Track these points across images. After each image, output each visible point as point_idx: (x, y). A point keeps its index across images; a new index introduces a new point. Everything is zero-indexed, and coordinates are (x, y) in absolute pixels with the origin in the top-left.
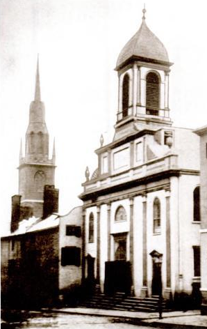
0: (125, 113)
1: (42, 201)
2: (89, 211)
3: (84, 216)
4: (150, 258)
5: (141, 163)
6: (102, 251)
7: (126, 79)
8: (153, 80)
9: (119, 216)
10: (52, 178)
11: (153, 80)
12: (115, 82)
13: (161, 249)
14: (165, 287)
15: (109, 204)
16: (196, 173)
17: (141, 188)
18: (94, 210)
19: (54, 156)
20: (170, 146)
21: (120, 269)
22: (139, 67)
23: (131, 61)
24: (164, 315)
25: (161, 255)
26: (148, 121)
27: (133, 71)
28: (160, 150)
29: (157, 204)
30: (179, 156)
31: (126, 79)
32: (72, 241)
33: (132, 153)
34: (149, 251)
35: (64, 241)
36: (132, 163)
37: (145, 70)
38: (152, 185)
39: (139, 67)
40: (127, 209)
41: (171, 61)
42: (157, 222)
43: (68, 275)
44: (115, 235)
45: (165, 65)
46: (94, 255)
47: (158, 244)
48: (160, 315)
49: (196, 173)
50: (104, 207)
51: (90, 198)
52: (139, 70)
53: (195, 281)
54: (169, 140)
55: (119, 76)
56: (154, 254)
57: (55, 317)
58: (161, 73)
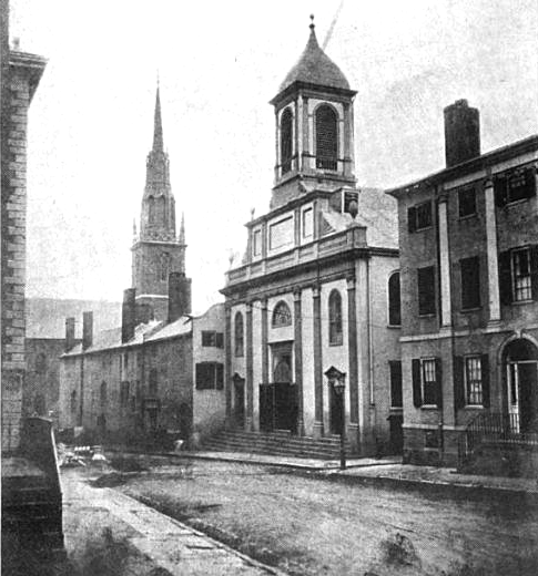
0: (286, 168)
1: (167, 297)
2: (235, 310)
3: (229, 318)
4: (325, 379)
5: (311, 240)
6: (259, 369)
7: (288, 114)
8: (327, 120)
9: (279, 317)
10: (180, 263)
11: (327, 120)
12: (269, 121)
13: (344, 367)
14: (348, 424)
15: (265, 300)
16: (393, 254)
17: (312, 276)
18: (243, 309)
19: (183, 231)
20: (354, 213)
21: (282, 401)
22: (306, 99)
23: (294, 90)
24: (348, 463)
25: (344, 375)
26: (319, 179)
27: (296, 104)
28: (339, 222)
29: (335, 298)
30: (369, 230)
31: (288, 114)
32: (210, 355)
33: (297, 226)
34: (325, 370)
35: (200, 354)
36: (297, 241)
37: (314, 104)
38: (324, 274)
39: (306, 99)
40: (344, 294)
41: (352, 88)
42: (336, 326)
43: (207, 405)
44: (276, 345)
45: (346, 95)
46: (243, 374)
47: (338, 358)
48: (343, 463)
49: (393, 254)
50: (258, 304)
51: (237, 291)
52: (306, 102)
53: (394, 413)
54: (352, 204)
55: (277, 113)
56: (332, 372)
57: (188, 466)
58: (338, 106)
